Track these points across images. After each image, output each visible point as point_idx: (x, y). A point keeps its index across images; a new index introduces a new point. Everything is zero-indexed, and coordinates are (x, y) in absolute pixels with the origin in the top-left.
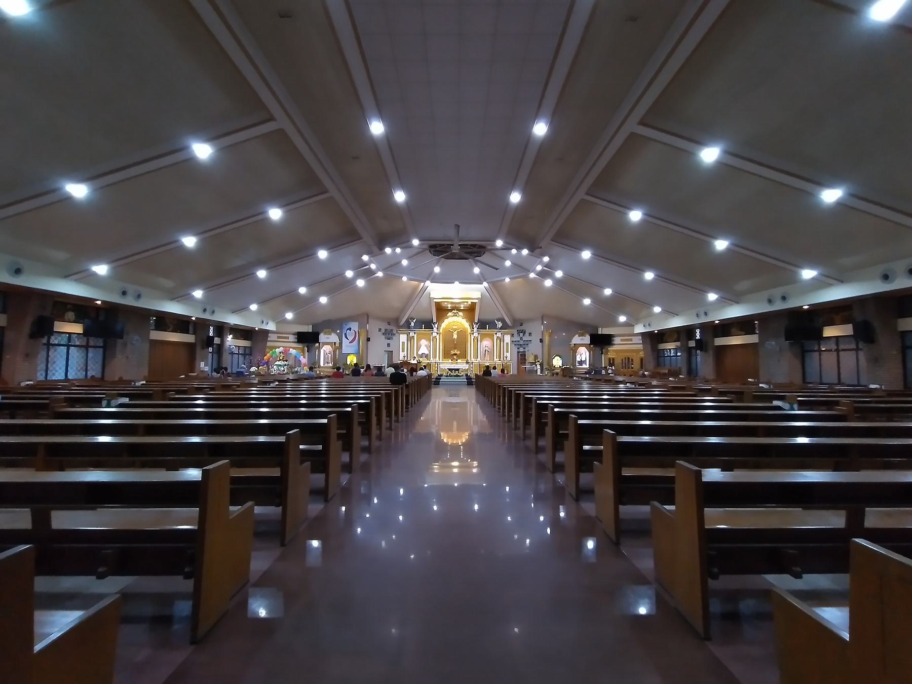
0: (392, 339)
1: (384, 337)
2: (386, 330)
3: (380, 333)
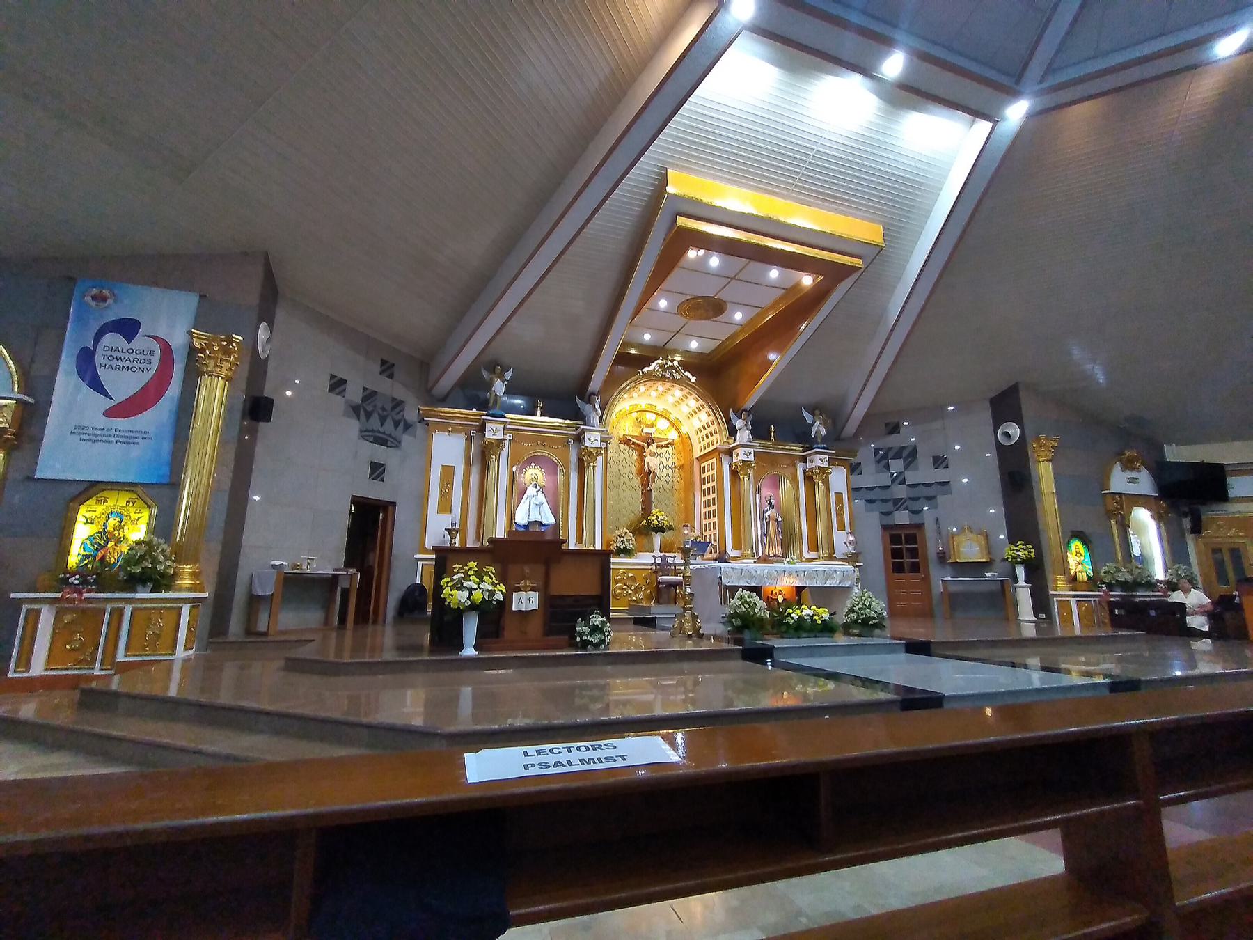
0: (397, 444)
1: (354, 426)
2: (369, 395)
3: (337, 401)
